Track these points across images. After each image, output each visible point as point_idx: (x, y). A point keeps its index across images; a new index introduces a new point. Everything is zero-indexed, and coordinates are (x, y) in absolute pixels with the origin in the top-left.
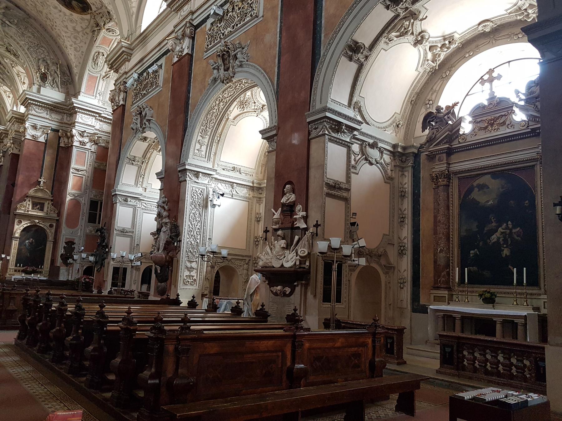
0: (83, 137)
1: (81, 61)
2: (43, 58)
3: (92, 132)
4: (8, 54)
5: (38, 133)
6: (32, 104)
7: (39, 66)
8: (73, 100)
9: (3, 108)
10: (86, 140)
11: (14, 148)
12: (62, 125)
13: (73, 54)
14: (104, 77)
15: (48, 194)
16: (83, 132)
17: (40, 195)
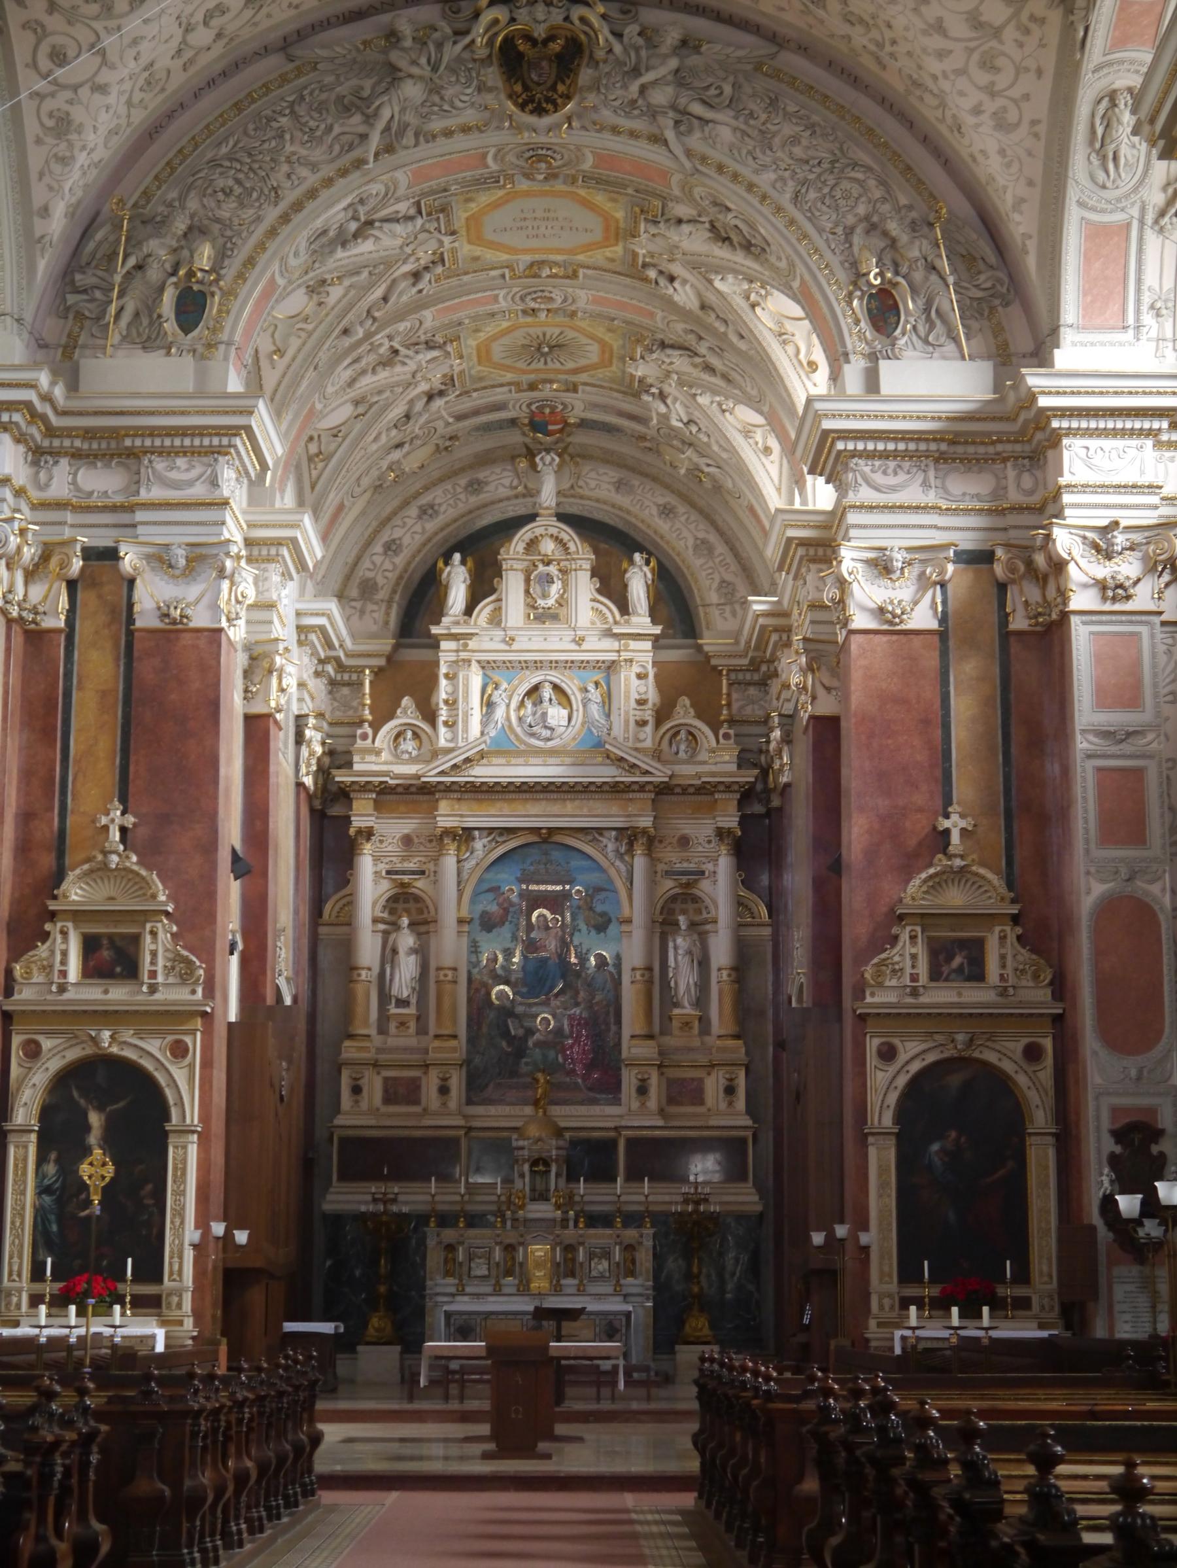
0: (1109, 557)
1: (1035, 168)
2: (867, 218)
3: (1149, 518)
4: (721, 252)
5: (899, 592)
6: (854, 454)
7: (855, 264)
8: (1031, 381)
9: (751, 509)
10: (1128, 568)
11: (821, 692)
12: (1000, 522)
13: (992, 146)
14: (1162, 214)
15: (987, 892)
16: (1105, 530)
17: (955, 898)
